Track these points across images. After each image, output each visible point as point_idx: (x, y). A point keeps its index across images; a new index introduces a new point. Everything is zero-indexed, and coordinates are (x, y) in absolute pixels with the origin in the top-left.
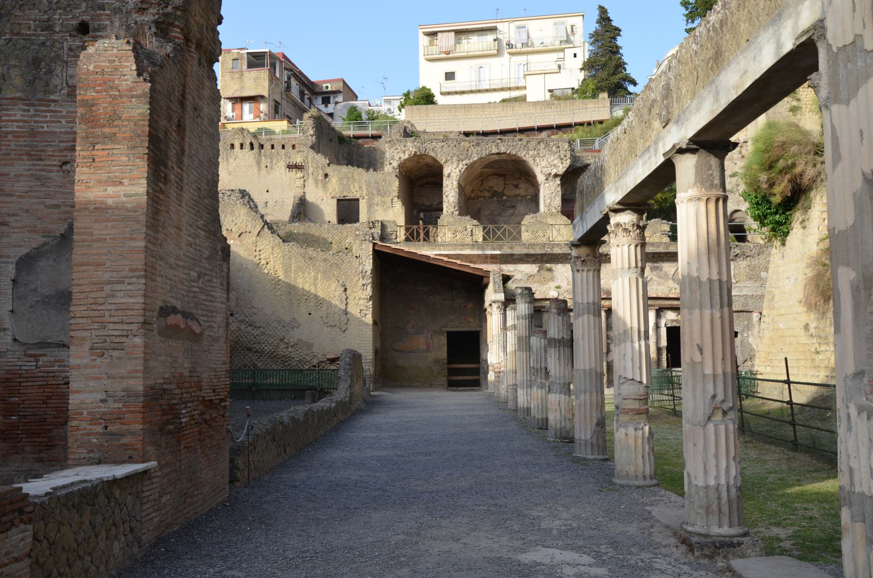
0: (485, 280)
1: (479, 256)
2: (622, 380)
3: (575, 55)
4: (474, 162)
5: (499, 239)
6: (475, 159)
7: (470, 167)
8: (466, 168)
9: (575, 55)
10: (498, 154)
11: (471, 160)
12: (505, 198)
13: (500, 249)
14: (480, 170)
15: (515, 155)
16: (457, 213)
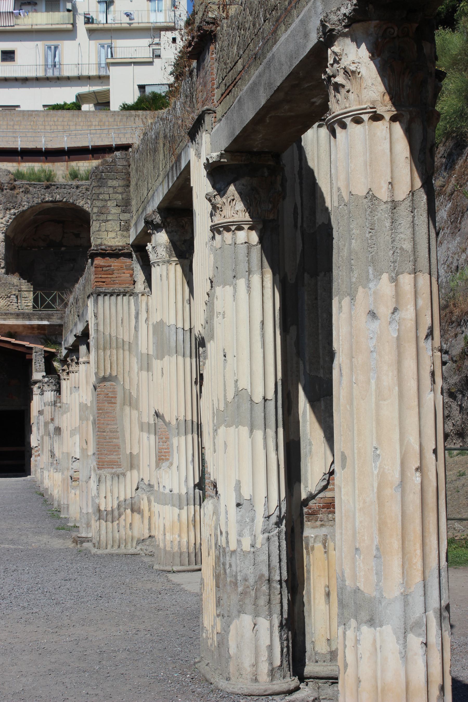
0: (28, 357)
1: (24, 326)
2: (74, 460)
3: (174, 40)
4: (24, 212)
5: (49, 306)
6: (26, 207)
7: (19, 218)
8: (14, 218)
9: (174, 40)
10: (52, 202)
11: (21, 209)
12: (63, 249)
13: (48, 317)
14: (32, 217)
15: (73, 204)
16: (3, 271)
